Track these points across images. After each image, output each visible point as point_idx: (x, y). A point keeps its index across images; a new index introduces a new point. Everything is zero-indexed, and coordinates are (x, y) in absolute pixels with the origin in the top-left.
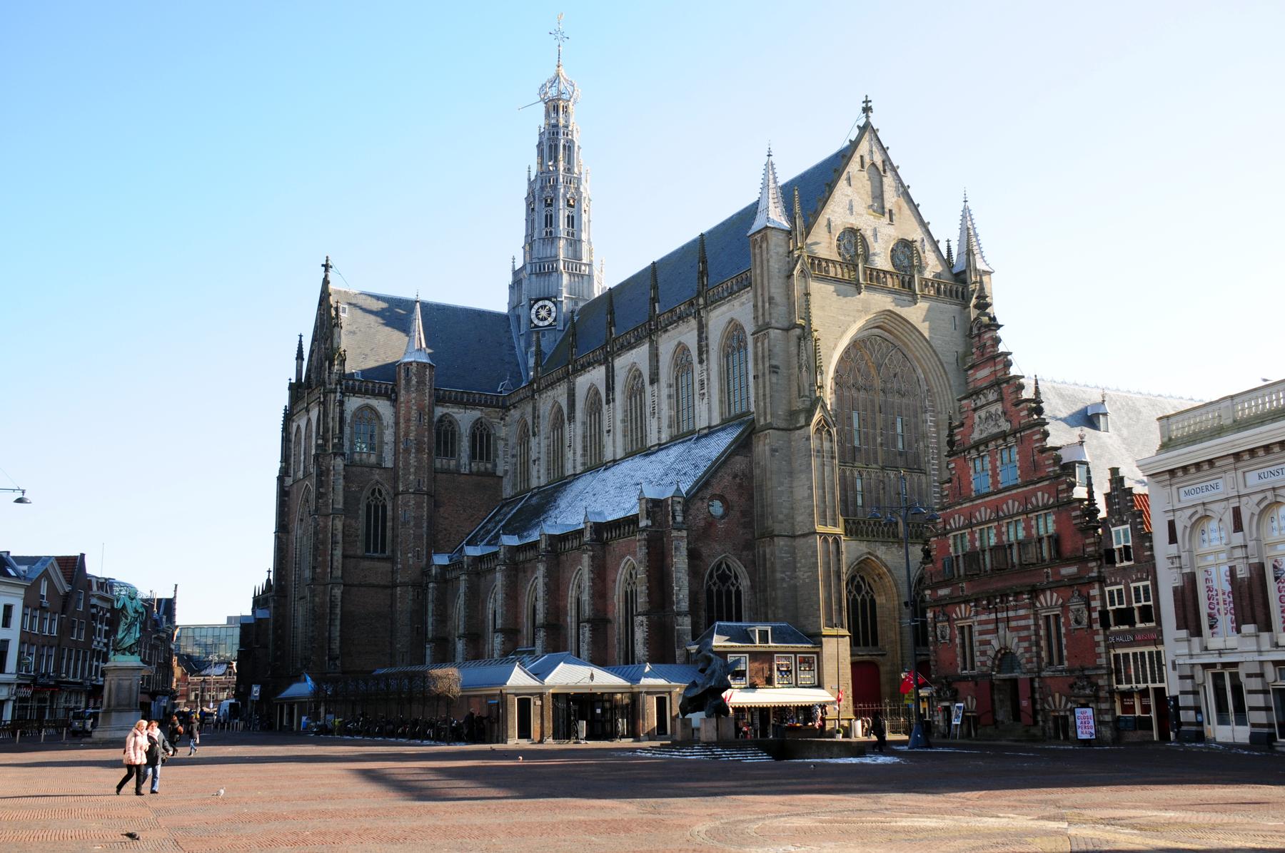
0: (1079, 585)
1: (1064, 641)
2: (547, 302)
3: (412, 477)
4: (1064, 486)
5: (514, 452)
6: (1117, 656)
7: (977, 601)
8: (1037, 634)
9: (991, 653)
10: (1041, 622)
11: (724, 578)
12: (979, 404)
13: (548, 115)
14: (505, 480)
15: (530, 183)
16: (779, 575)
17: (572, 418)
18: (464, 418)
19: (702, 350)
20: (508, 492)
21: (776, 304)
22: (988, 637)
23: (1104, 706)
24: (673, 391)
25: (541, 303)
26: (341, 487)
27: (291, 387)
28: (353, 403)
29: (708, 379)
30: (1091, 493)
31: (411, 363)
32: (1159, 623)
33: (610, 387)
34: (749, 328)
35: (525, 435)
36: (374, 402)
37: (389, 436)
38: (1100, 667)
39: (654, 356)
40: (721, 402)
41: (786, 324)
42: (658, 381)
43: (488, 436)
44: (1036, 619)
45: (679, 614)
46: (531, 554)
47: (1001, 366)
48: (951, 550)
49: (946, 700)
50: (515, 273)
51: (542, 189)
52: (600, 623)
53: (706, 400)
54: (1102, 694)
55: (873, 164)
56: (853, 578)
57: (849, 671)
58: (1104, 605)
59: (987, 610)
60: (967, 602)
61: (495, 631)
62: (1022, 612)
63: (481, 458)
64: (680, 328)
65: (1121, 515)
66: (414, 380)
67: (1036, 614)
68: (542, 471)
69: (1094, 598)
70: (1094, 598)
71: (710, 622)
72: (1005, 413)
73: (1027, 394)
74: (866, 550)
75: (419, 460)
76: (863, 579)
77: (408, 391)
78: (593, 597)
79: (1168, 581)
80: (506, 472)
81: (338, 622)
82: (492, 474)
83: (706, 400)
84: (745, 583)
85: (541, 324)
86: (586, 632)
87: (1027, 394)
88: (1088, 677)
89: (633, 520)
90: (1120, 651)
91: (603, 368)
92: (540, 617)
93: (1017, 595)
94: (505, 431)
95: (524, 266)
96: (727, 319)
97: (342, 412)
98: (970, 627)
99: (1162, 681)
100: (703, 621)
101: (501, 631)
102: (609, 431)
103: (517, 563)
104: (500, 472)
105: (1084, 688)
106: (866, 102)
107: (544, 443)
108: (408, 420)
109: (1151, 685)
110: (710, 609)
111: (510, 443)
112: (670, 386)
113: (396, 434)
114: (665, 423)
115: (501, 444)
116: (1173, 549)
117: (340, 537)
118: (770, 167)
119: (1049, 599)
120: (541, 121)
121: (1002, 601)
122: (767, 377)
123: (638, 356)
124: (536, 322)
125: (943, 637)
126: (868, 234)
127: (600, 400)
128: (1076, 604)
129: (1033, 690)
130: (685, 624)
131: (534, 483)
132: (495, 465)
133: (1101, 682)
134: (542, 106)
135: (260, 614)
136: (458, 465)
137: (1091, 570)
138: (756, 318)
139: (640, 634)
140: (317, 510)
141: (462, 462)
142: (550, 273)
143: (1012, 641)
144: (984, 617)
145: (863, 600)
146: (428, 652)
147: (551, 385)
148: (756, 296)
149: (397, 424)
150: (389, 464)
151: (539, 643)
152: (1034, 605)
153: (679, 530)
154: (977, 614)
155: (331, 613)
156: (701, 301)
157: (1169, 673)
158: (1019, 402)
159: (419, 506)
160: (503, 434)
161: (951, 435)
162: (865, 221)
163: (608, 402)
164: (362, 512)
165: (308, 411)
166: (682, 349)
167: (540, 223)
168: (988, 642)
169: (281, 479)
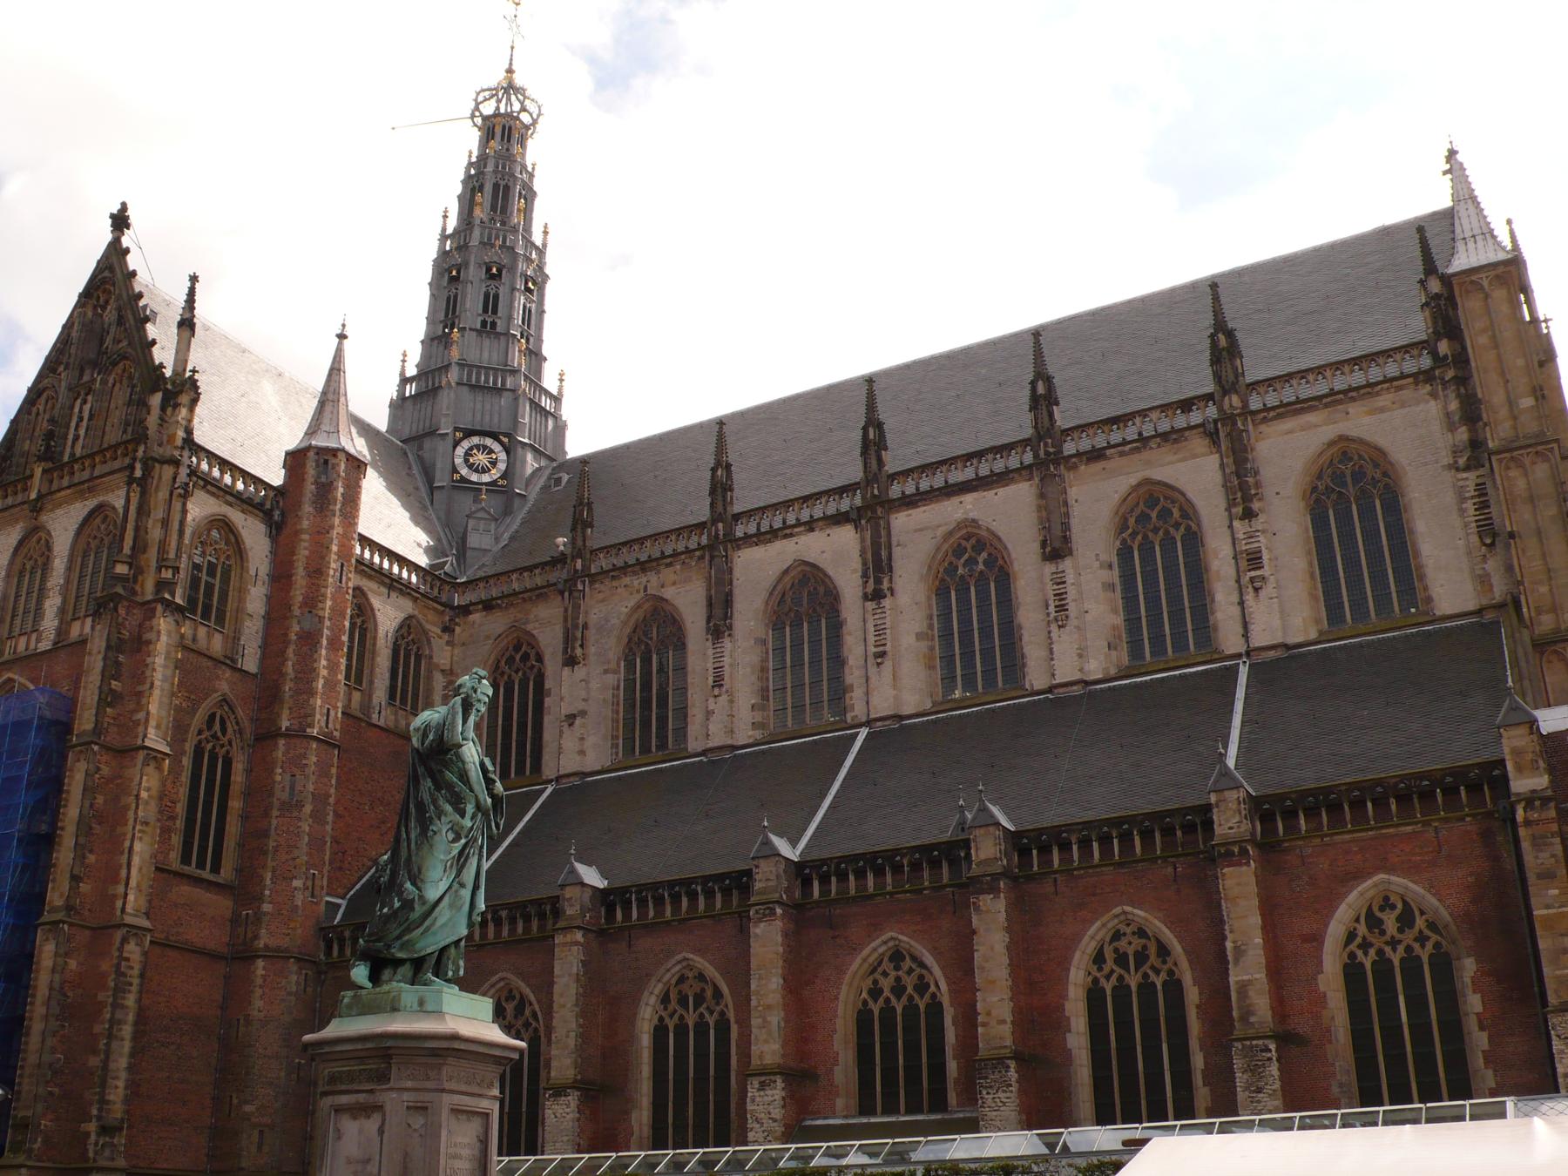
2: (489, 442)
15: (444, 237)
25: (476, 440)
31: (334, 452)
33: (878, 566)
36: (236, 516)
42: (1071, 554)
43: (418, 657)
63: (404, 701)
64: (1146, 455)
68: (591, 740)
75: (333, 667)
81: (127, 1031)
85: (474, 477)
97: (184, 512)
136: (366, 706)
141: (375, 701)
142: (498, 391)
150: (251, 664)
155: (115, 1006)
165: (37, 507)
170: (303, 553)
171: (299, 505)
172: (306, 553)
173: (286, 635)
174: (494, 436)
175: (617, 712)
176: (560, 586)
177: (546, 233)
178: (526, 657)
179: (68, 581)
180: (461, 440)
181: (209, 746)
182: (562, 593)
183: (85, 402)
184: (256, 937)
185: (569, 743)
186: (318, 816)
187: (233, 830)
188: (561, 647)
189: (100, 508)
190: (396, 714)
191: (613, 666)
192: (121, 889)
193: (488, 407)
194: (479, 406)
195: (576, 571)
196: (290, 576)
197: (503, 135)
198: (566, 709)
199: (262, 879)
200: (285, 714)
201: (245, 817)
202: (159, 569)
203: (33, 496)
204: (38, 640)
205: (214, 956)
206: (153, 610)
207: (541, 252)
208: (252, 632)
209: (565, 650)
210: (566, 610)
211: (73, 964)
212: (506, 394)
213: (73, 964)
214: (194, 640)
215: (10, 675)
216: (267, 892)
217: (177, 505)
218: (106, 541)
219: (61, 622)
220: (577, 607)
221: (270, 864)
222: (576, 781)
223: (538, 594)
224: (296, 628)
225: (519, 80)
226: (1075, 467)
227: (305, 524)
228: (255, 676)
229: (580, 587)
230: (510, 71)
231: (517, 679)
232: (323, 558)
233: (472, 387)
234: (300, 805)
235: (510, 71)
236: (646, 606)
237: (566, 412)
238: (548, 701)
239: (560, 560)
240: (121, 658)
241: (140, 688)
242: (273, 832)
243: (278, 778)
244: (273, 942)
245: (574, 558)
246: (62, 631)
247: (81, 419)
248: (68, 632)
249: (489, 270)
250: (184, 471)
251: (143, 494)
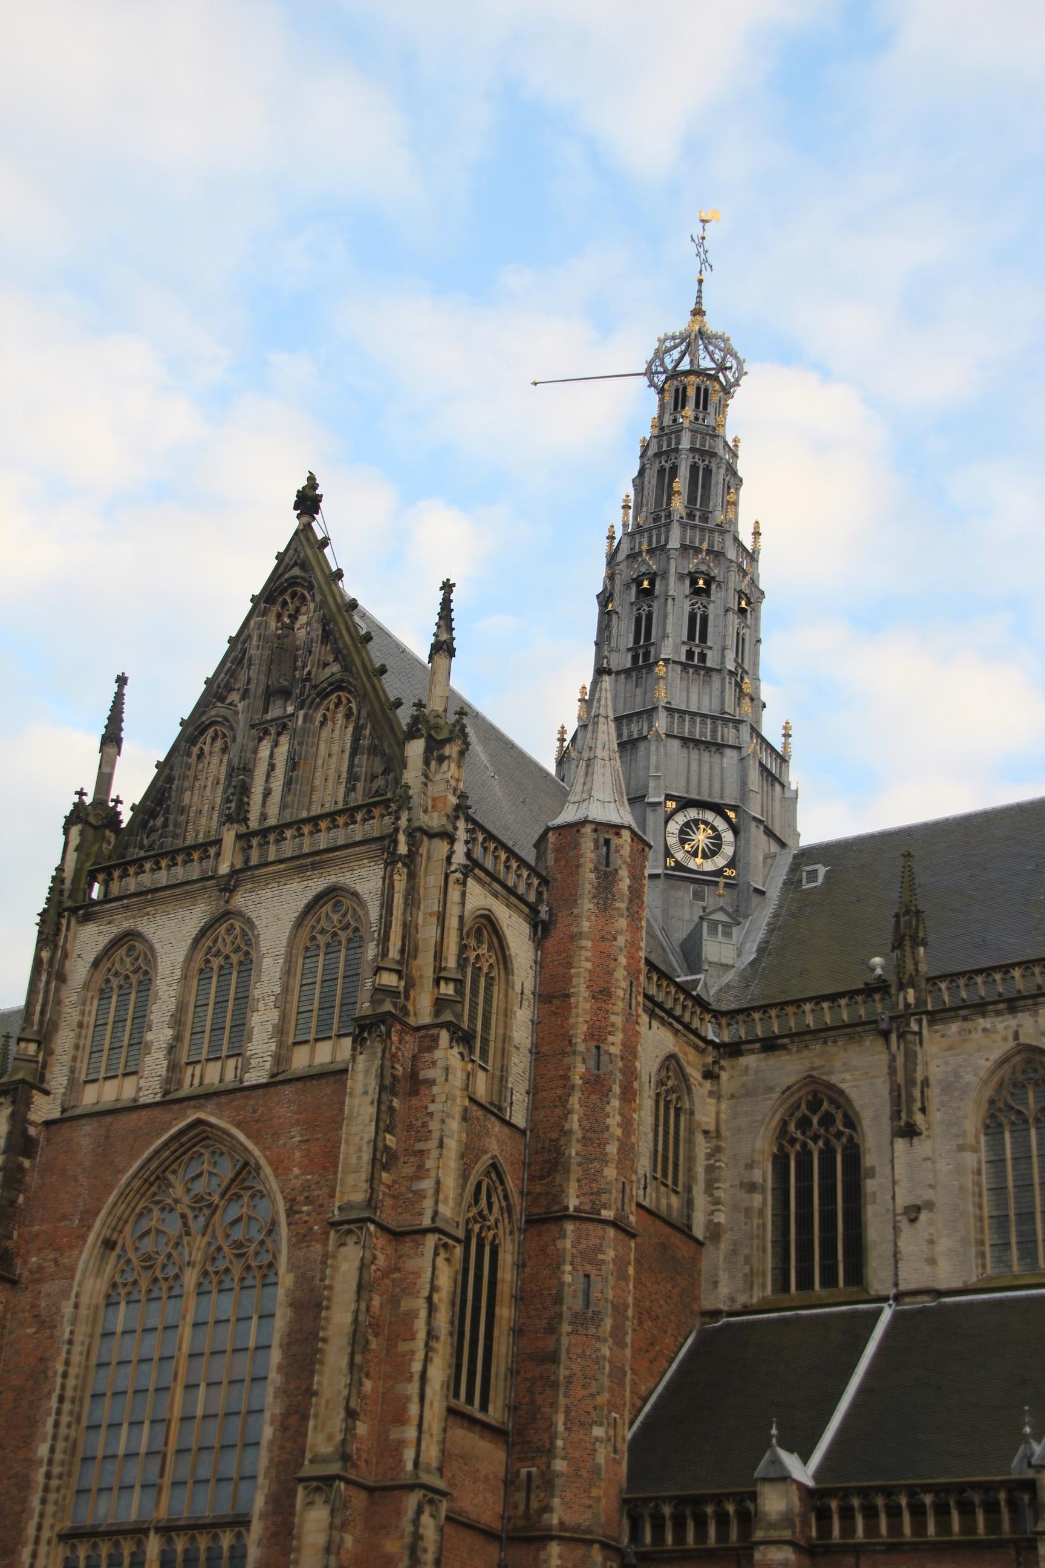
2: (710, 816)
5: (757, 1176)
13: (680, 400)
14: (715, 1257)
25: (693, 813)
68: (944, 1244)
80: (715, 1232)
82: (685, 1230)
104: (699, 1232)
115: (702, 1146)
132: (689, 1204)
140: (371, 1203)
142: (720, 747)
149: (552, 996)
165: (229, 885)
170: (584, 964)
171: (572, 900)
172: (589, 965)
173: (566, 1077)
174: (718, 809)
175: (980, 1207)
176: (884, 1026)
177: (757, 534)
178: (827, 1120)
179: (286, 989)
180: (675, 812)
181: (477, 1227)
182: (885, 1035)
183: (276, 744)
184: (547, 1509)
185: (911, 1242)
187: (503, 1349)
188: (887, 1110)
189: (331, 894)
190: (657, 1190)
191: (970, 1140)
192: (411, 1433)
193: (706, 769)
194: (694, 767)
195: (907, 1005)
196: (568, 996)
198: (903, 1199)
199: (552, 1425)
200: (572, 1188)
201: (518, 1332)
202: (437, 982)
203: (224, 869)
204: (246, 1068)
205: (489, 1535)
206: (435, 1039)
207: (753, 557)
209: (896, 1115)
210: (893, 1059)
211: (349, 1540)
212: (729, 752)
213: (349, 1540)
215: (202, 1115)
216: (559, 1443)
217: (454, 895)
218: (343, 936)
219: (280, 1044)
220: (910, 1058)
221: (562, 1400)
222: (929, 1302)
223: (851, 1031)
224: (581, 1068)
225: (713, 324)
227: (586, 925)
228: (523, 1132)
229: (914, 1027)
230: (698, 312)
231: (815, 1149)
232: (610, 973)
233: (686, 741)
234: (596, 1319)
235: (698, 312)
236: (1017, 1059)
237: (795, 777)
238: (870, 1185)
239: (879, 988)
240: (396, 1103)
241: (420, 1146)
242: (563, 1356)
243: (568, 1279)
244: (571, 1519)
245: (902, 987)
246: (280, 1059)
247: (272, 767)
248: (289, 1060)
249: (694, 582)
250: (460, 848)
251: (412, 876)
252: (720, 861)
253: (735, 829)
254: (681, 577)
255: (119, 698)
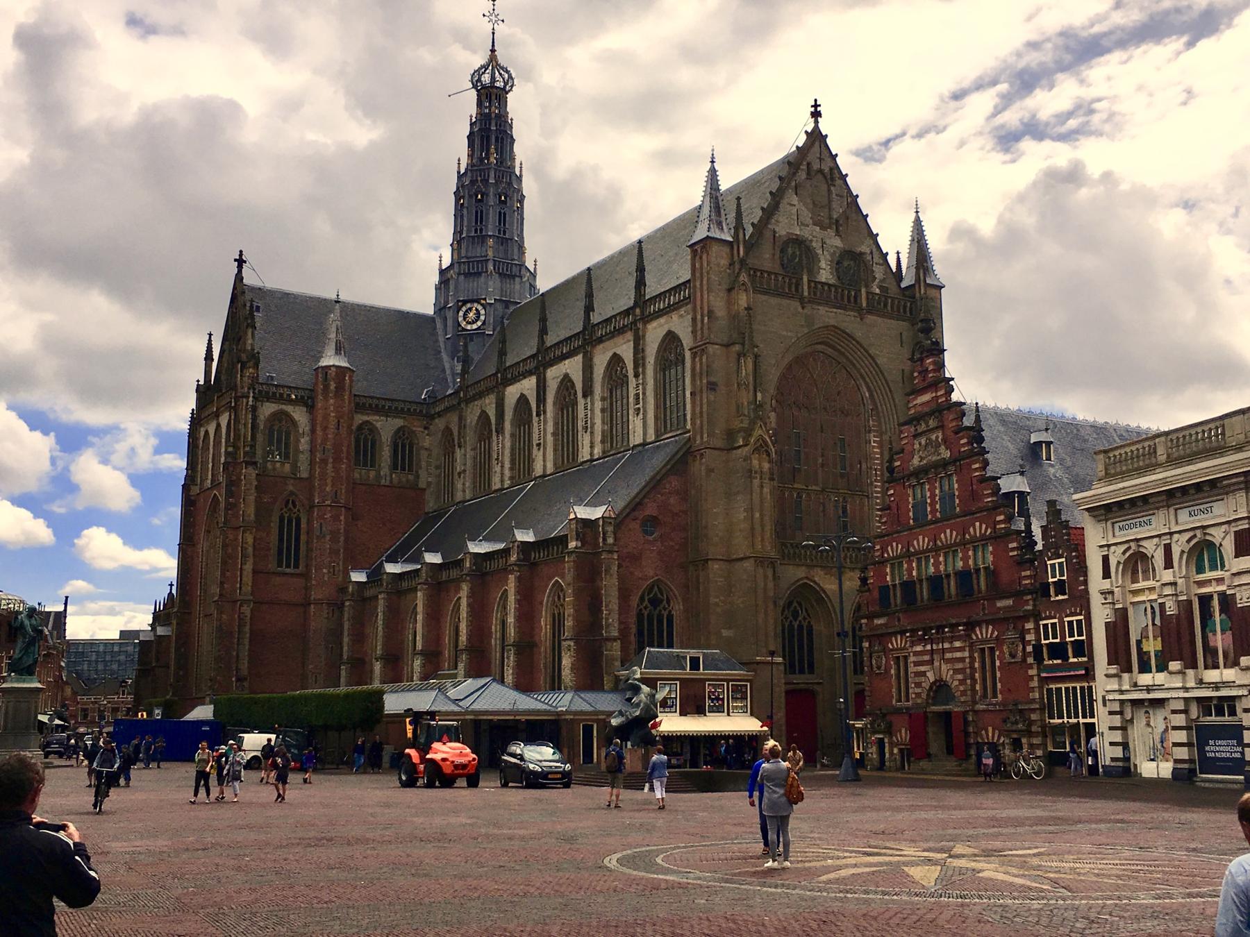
0: (1015, 620)
1: (998, 675)
3: (328, 489)
4: (1002, 517)
6: (1049, 691)
7: (913, 631)
8: (972, 667)
9: (926, 685)
10: (976, 655)
11: (655, 602)
12: (920, 430)
13: (480, 104)
15: (460, 176)
16: (713, 600)
17: (500, 430)
18: (386, 427)
19: (639, 360)
20: (431, 505)
21: (717, 318)
22: (922, 669)
23: (1036, 741)
24: (607, 404)
25: (469, 305)
26: (252, 498)
27: (199, 389)
28: (268, 409)
29: (644, 394)
30: (1028, 525)
31: (328, 367)
32: (1091, 658)
33: (541, 399)
34: (687, 341)
35: (449, 443)
36: (289, 408)
37: (304, 444)
38: (1034, 701)
39: (588, 368)
40: (656, 418)
41: (725, 340)
44: (971, 652)
45: (608, 639)
46: (454, 573)
47: (942, 392)
48: (888, 578)
49: (879, 733)
50: (442, 272)
51: (473, 182)
52: (526, 647)
53: (641, 416)
54: (1034, 729)
55: (821, 171)
56: (790, 603)
57: (783, 700)
58: (1038, 639)
59: (922, 640)
60: (903, 633)
61: (415, 653)
62: (957, 644)
65: (1057, 548)
66: (333, 386)
67: (971, 646)
68: (467, 484)
69: (1028, 631)
70: (1028, 631)
71: (641, 649)
72: (945, 440)
73: (968, 421)
74: (803, 575)
75: (336, 470)
76: (800, 604)
77: (326, 398)
78: (519, 618)
79: (1101, 615)
80: (429, 484)
81: (246, 642)
82: (414, 487)
83: (641, 416)
84: (677, 608)
85: (469, 327)
86: (511, 659)
87: (968, 421)
88: (1021, 711)
89: (562, 540)
90: (1053, 686)
91: (533, 380)
92: (463, 638)
93: (953, 627)
94: (428, 441)
95: (452, 265)
96: (661, 333)
97: (255, 418)
98: (906, 658)
99: (1092, 716)
100: (633, 646)
101: (422, 653)
102: (539, 445)
103: (439, 584)
104: (422, 485)
105: (1016, 723)
106: (816, 106)
107: (470, 454)
108: (325, 429)
109: (1082, 721)
110: (640, 633)
111: (435, 452)
112: (603, 399)
113: (312, 442)
114: (598, 438)
115: (424, 454)
116: (1106, 584)
117: (250, 550)
118: (713, 173)
119: (985, 633)
120: (473, 110)
121: (937, 633)
122: (705, 396)
123: (572, 367)
124: (463, 324)
125: (879, 668)
126: (816, 245)
127: (530, 410)
128: (1011, 635)
129: (966, 722)
130: (615, 649)
131: (459, 496)
132: (418, 477)
133: (1034, 717)
134: (474, 92)
135: (161, 631)
136: (378, 476)
137: (1027, 602)
138: (694, 332)
139: (566, 661)
142: (479, 274)
143: (946, 672)
144: (919, 648)
145: (801, 627)
146: (343, 673)
147: (480, 395)
148: (694, 309)
149: (313, 431)
151: (461, 666)
152: (969, 636)
153: (610, 552)
154: (913, 644)
155: (239, 632)
156: (638, 311)
157: (1099, 709)
158: (960, 430)
159: (336, 518)
160: (426, 444)
161: (891, 461)
162: (811, 233)
163: (538, 415)
164: (275, 526)
165: (217, 415)
166: (616, 360)
167: (469, 221)
168: (924, 674)
169: (186, 488)
174: (478, 301)
186: (334, 539)
197: (492, 95)
208: (304, 459)
214: (274, 469)
226: (594, 346)
230: (493, 51)
234: (324, 536)
235: (493, 51)
252: (479, 323)
253: (485, 308)
254: (470, 196)
255: (210, 340)
